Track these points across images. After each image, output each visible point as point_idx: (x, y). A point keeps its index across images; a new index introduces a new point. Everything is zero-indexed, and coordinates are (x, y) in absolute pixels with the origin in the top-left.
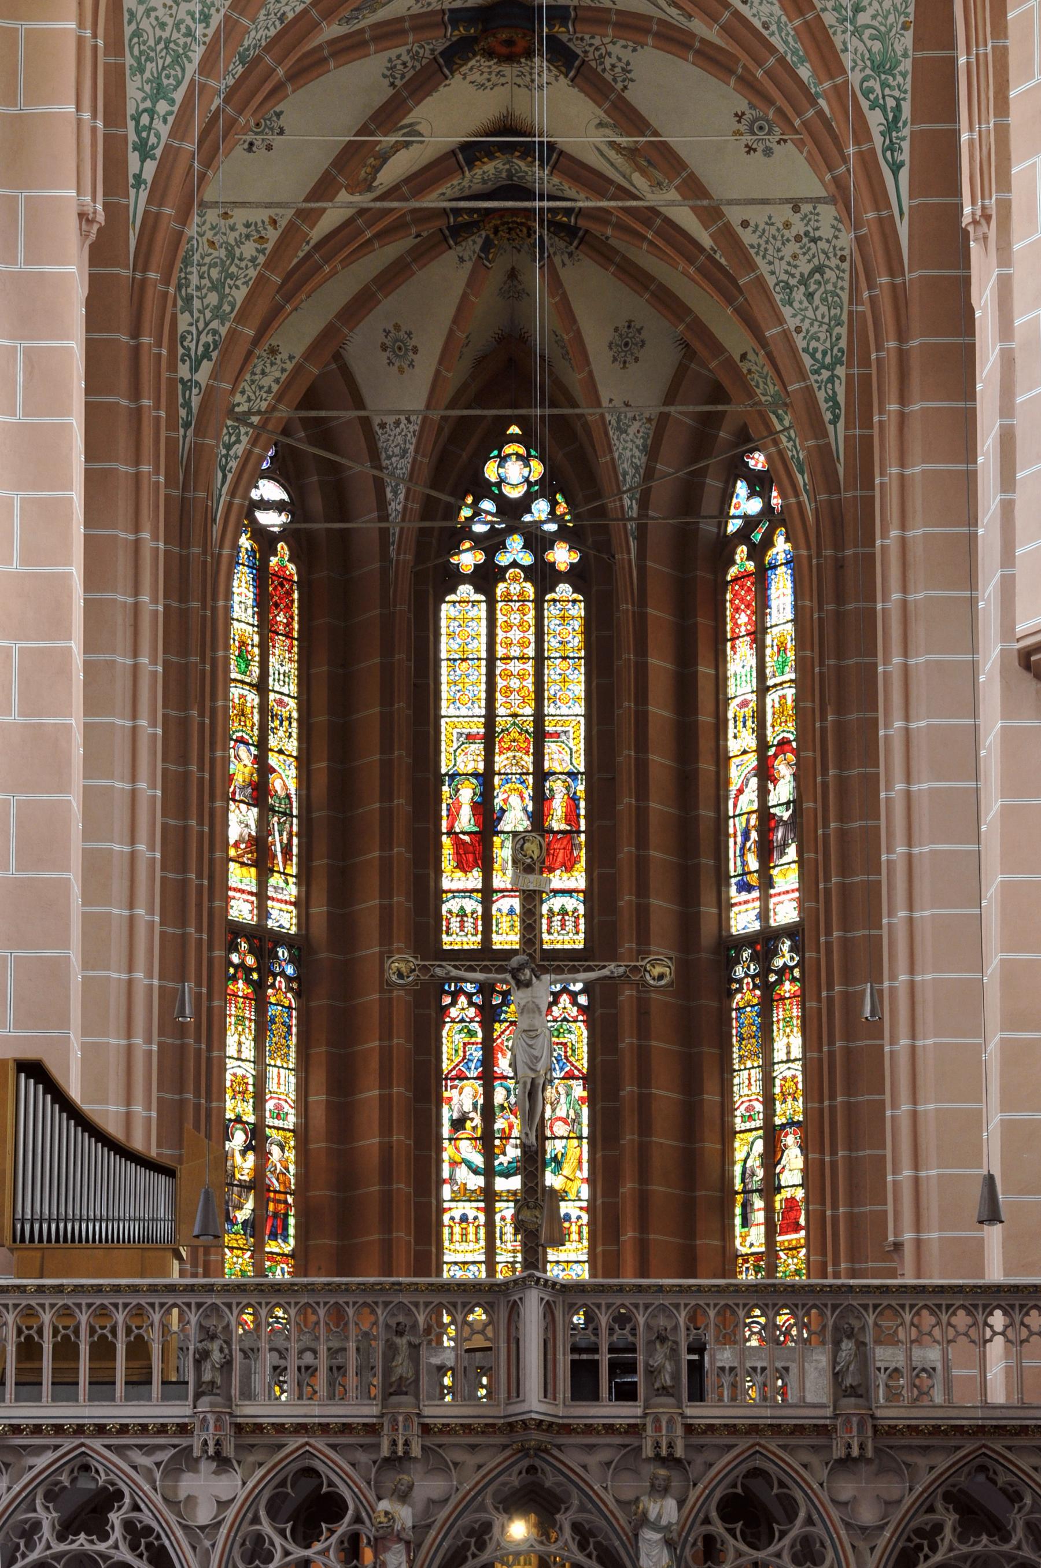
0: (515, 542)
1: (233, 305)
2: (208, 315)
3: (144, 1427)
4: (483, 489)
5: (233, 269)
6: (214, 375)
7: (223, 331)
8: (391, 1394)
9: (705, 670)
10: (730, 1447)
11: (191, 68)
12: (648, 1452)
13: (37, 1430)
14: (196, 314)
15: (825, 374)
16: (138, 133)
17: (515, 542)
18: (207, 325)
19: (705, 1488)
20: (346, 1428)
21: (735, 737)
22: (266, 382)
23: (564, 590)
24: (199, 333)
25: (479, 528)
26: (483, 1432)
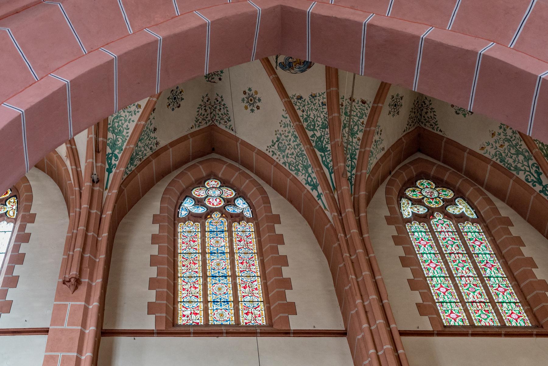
1: (527, 151)
2: (526, 163)
5: (514, 142)
14: (523, 168)
16: (310, 185)
18: (529, 166)
21: (441, 131)
24: (530, 172)
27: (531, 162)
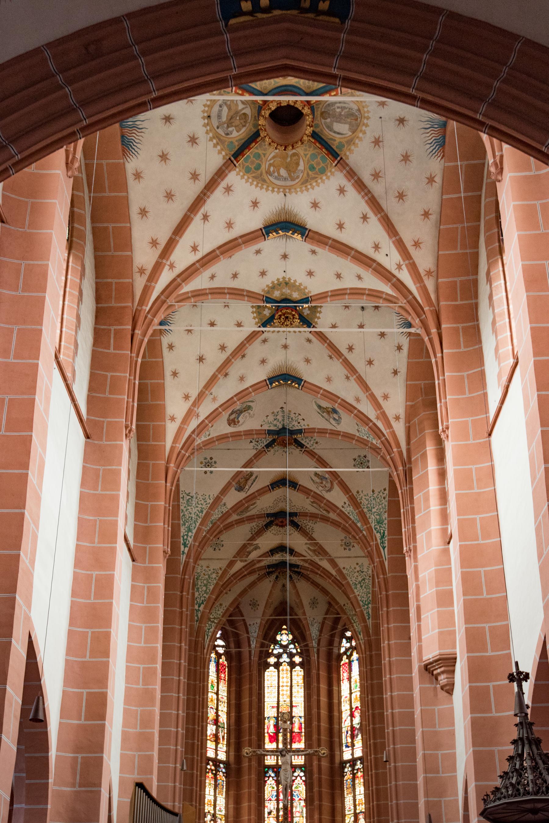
0: (285, 656)
4: (276, 642)
6: (205, 608)
7: (207, 597)
9: (335, 688)
11: (198, 524)
15: (366, 607)
17: (285, 656)
22: (219, 613)
23: (298, 668)
25: (275, 652)
27: (205, 595)
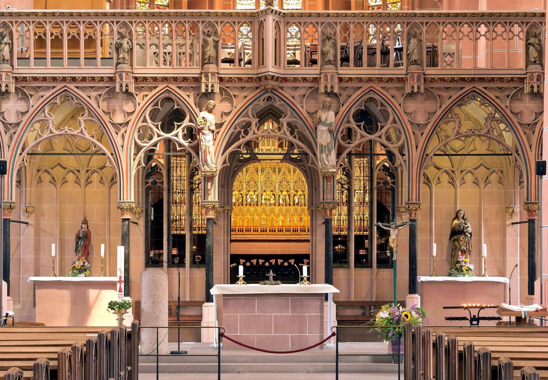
3: (93, 79)
8: (205, 64)
10: (359, 88)
12: (322, 90)
13: (45, 79)
19: (348, 107)
20: (185, 79)
26: (247, 81)
